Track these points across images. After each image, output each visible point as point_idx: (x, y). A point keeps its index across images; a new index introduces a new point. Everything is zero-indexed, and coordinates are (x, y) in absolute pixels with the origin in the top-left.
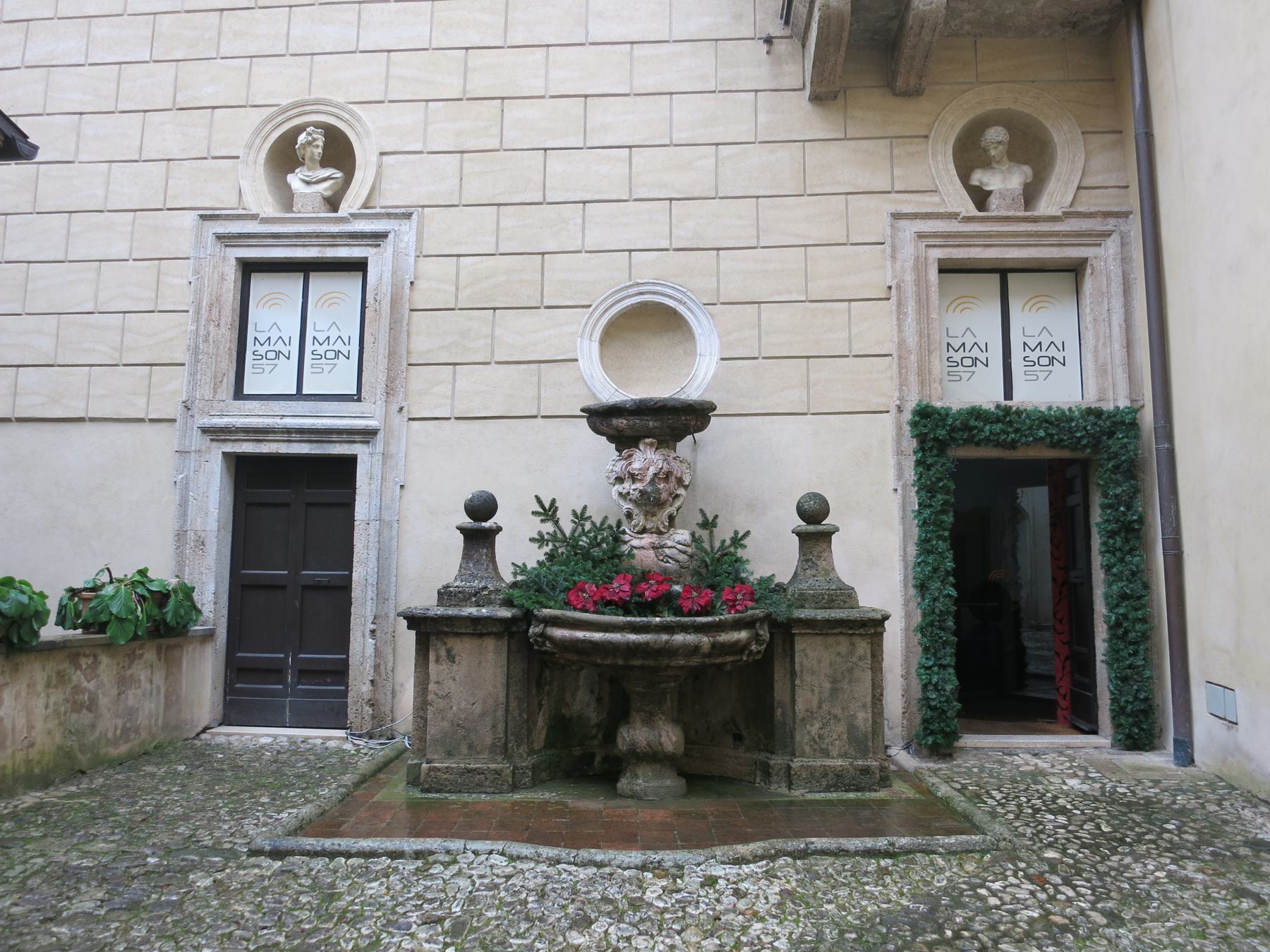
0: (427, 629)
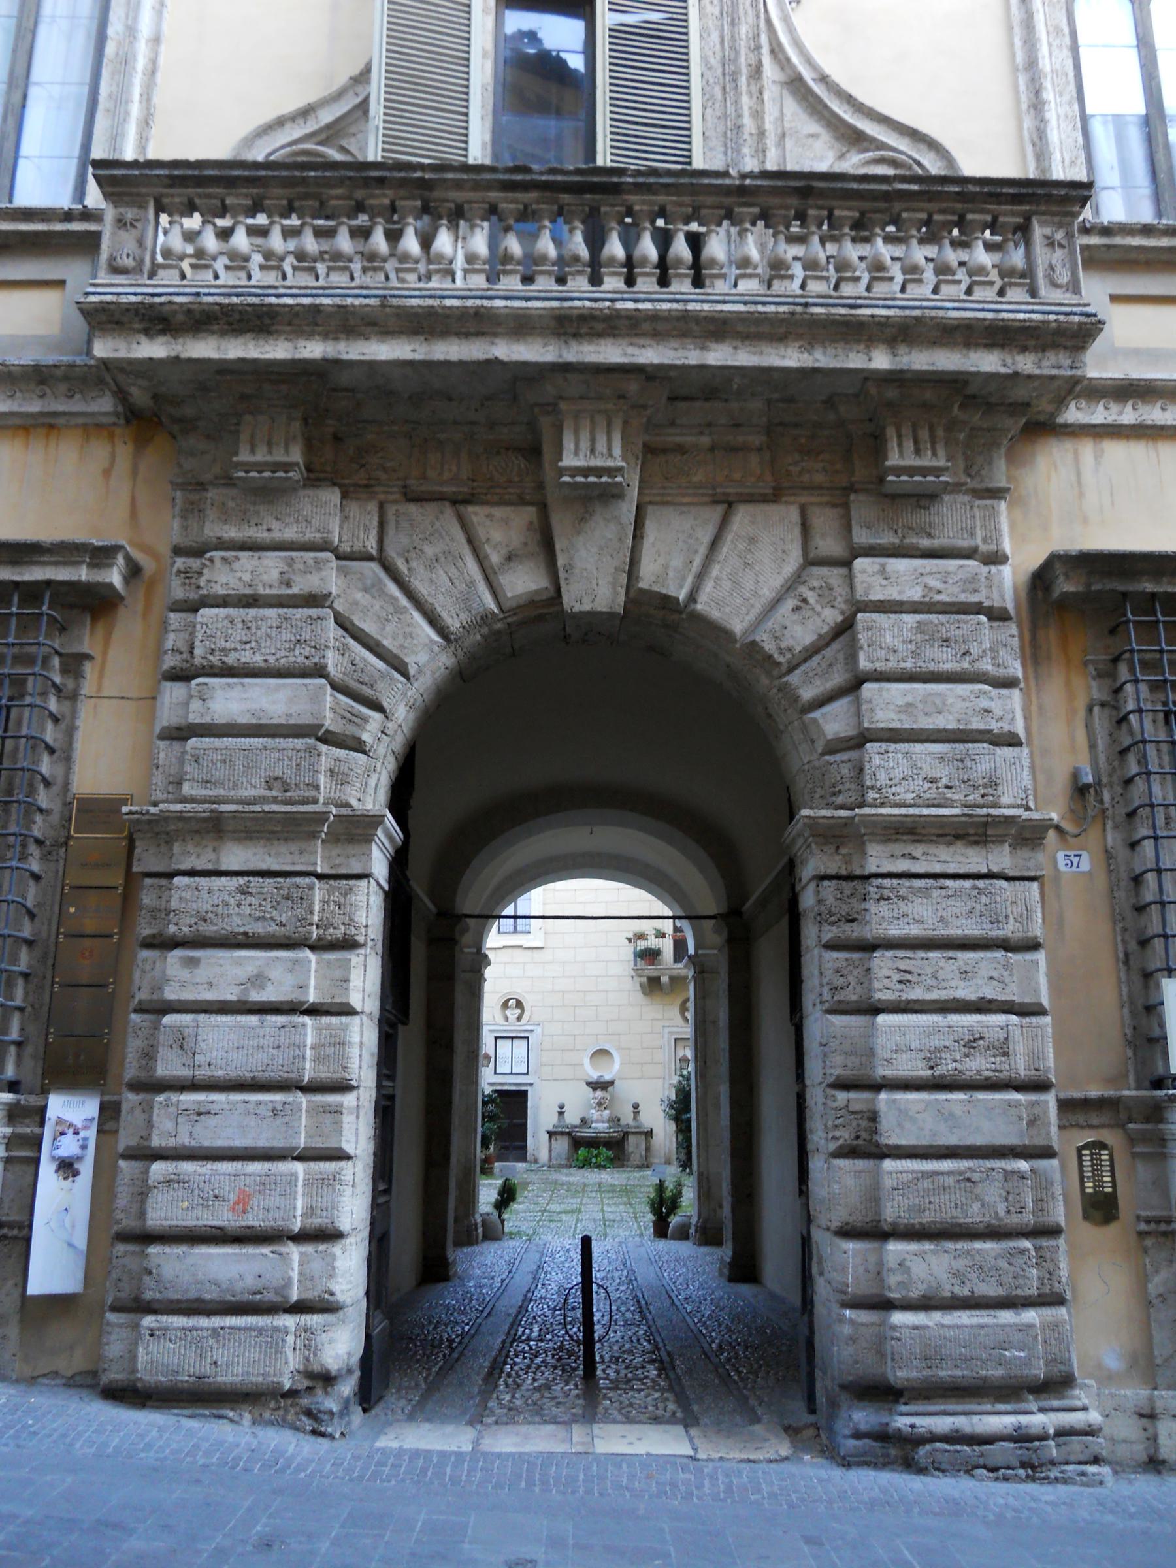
0: (551, 1134)
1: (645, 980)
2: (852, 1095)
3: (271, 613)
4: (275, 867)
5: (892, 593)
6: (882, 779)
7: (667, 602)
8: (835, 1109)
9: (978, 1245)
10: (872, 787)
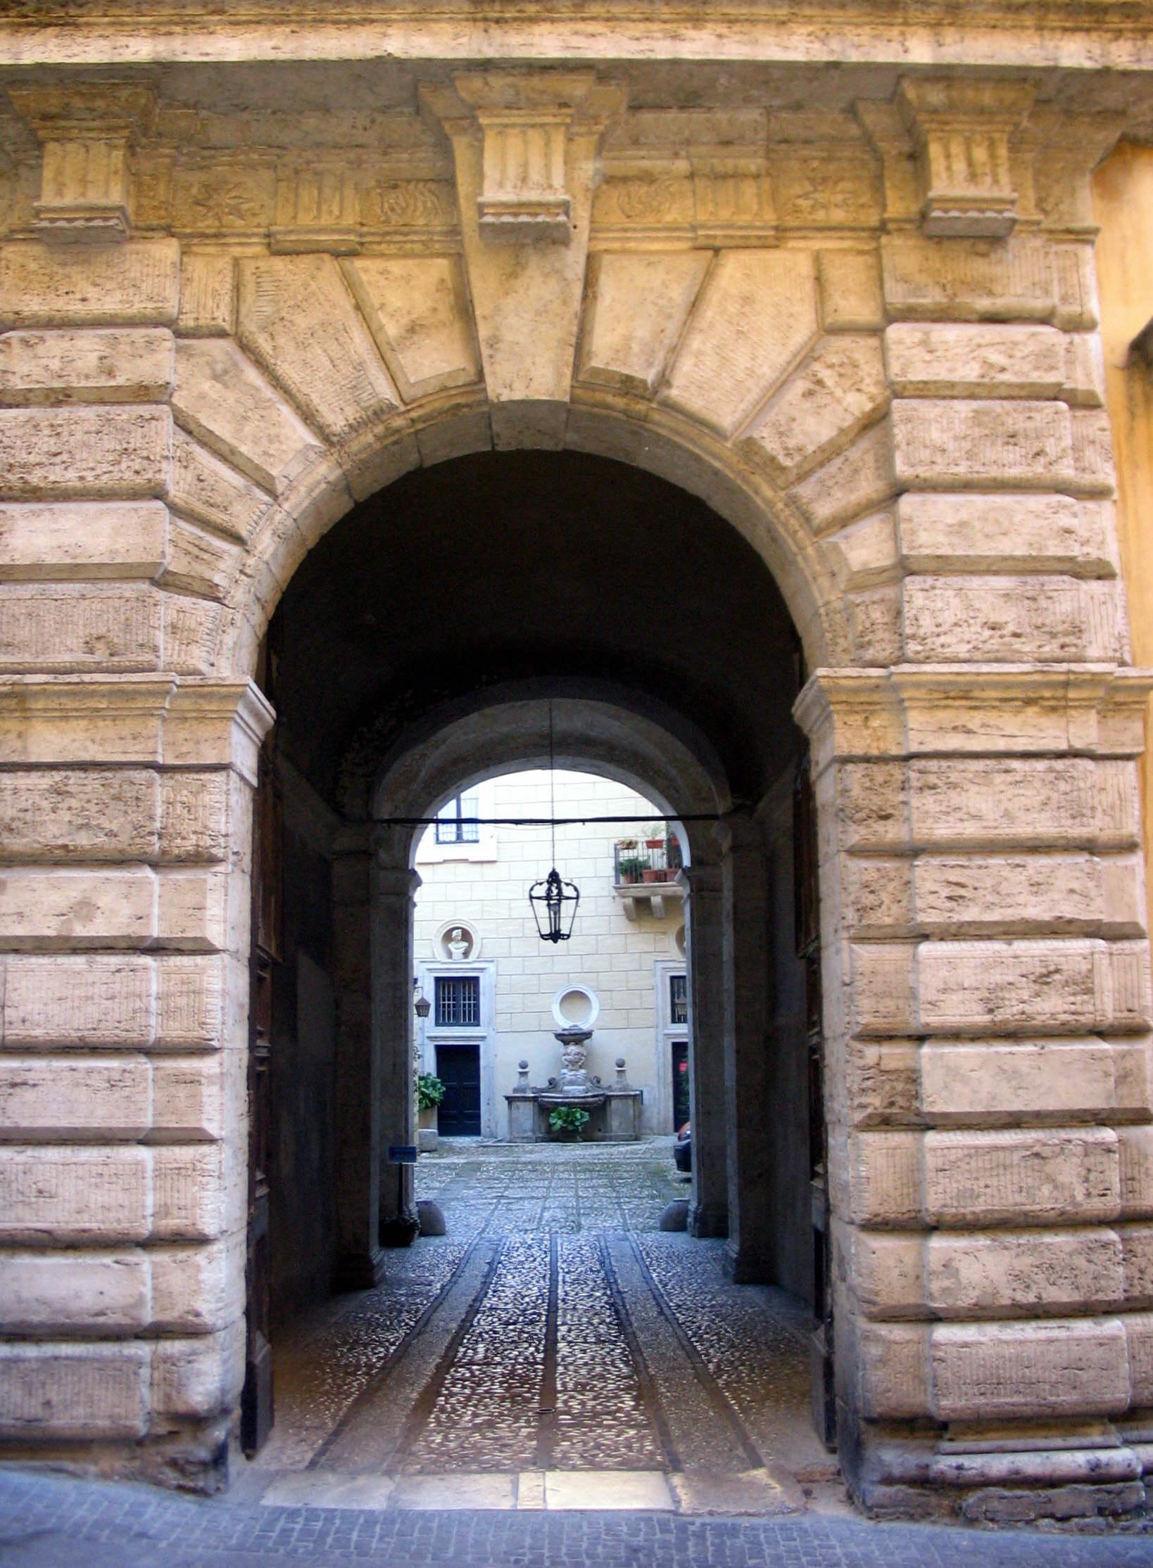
0: (510, 1100)
1: (629, 901)
2: (886, 1049)
3: (89, 414)
4: (101, 757)
5: (940, 372)
6: (927, 624)
7: (628, 385)
8: (863, 1068)
9: (1048, 1238)
10: (913, 637)
